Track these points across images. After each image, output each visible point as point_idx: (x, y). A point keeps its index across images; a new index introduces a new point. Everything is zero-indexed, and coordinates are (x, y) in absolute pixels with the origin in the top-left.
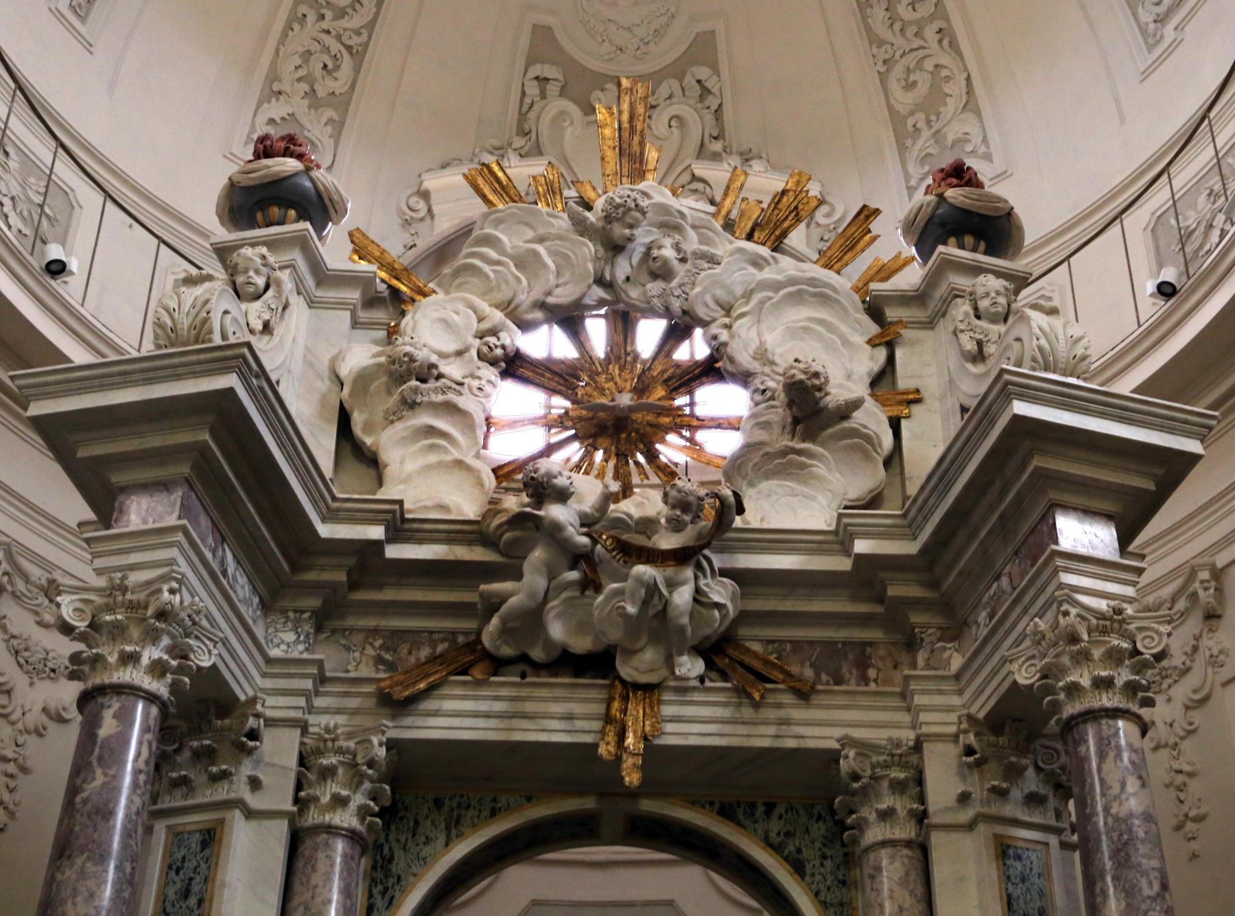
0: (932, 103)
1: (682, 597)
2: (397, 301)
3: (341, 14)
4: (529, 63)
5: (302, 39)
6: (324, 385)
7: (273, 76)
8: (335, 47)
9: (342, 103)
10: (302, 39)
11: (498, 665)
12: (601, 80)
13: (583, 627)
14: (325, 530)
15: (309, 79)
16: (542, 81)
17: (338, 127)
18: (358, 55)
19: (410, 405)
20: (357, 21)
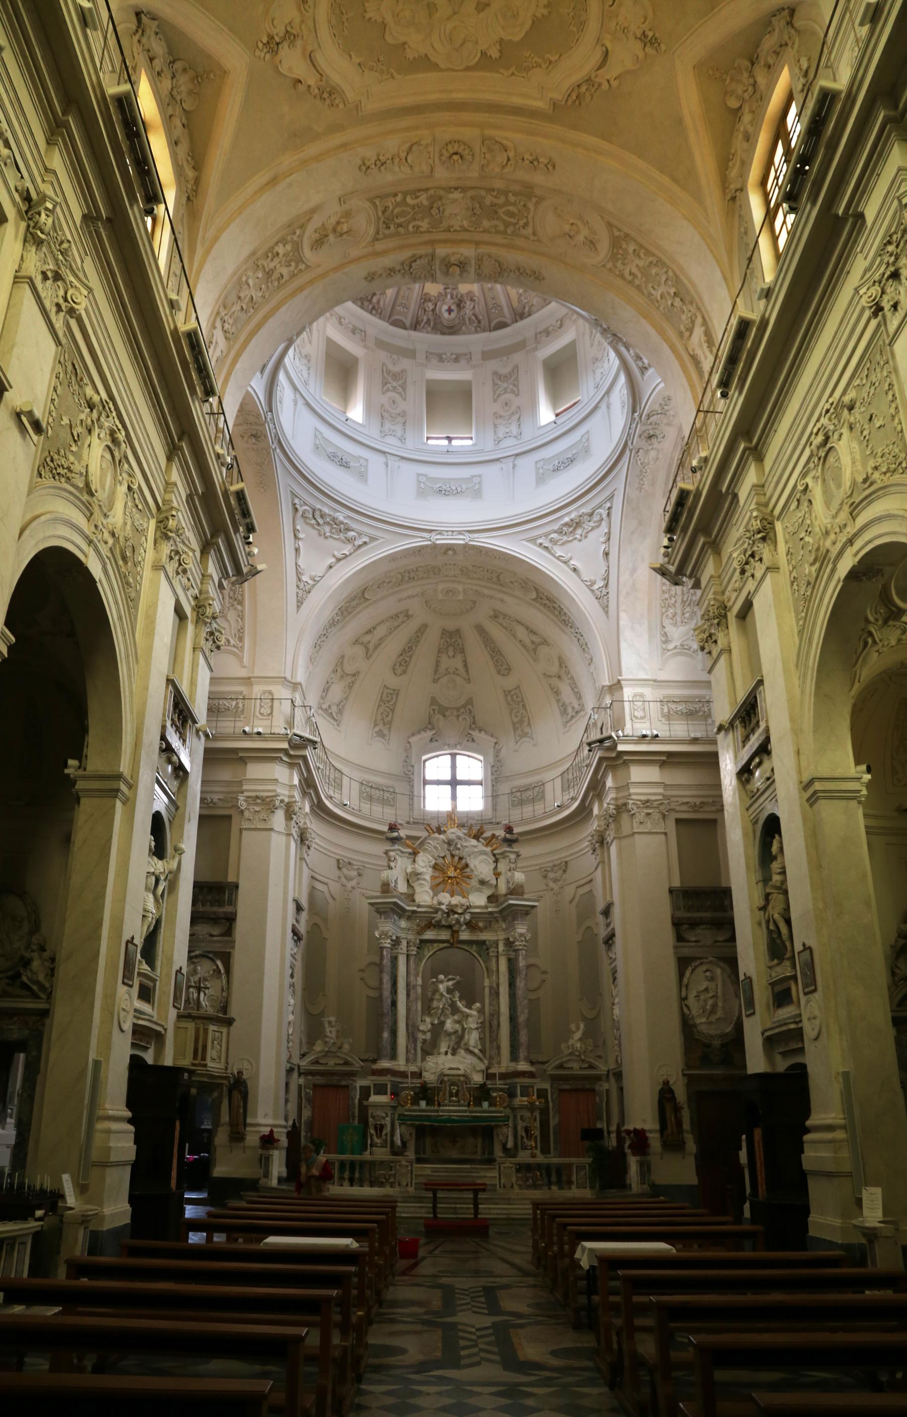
0: (521, 722)
1: (462, 920)
2: (415, 854)
3: (389, 702)
4: (431, 704)
5: (381, 710)
6: (404, 874)
7: (376, 721)
8: (388, 710)
9: (390, 723)
10: (381, 710)
11: (435, 926)
12: (447, 709)
13: (447, 921)
14: (408, 908)
15: (383, 719)
16: (434, 710)
17: (390, 729)
18: (393, 711)
19: (419, 879)
20: (392, 702)
